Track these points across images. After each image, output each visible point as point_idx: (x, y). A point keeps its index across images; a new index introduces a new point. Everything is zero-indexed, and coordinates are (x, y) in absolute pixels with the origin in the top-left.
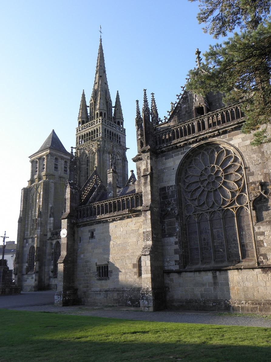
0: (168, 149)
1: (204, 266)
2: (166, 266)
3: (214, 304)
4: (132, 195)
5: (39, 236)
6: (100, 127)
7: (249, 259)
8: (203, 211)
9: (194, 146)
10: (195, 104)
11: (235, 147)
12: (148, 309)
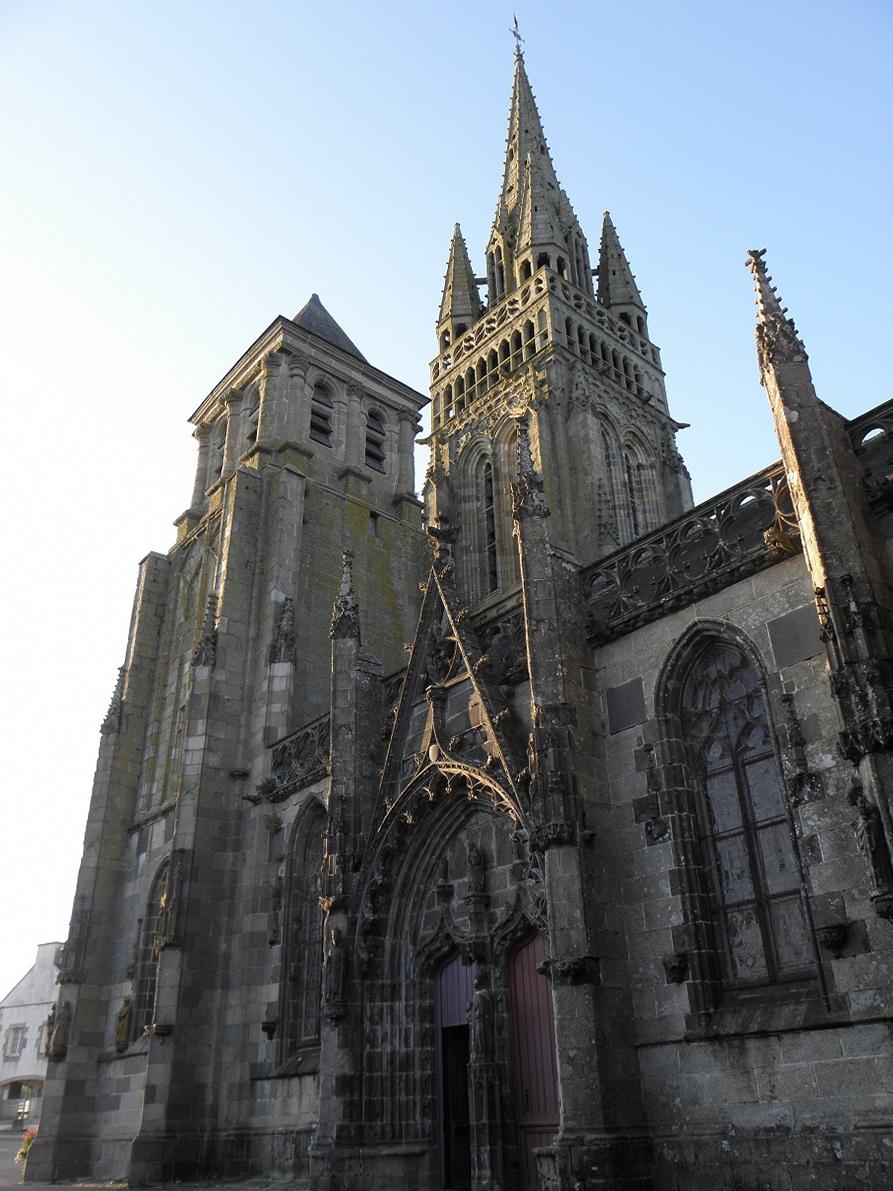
5: (196, 779)
6: (541, 310)
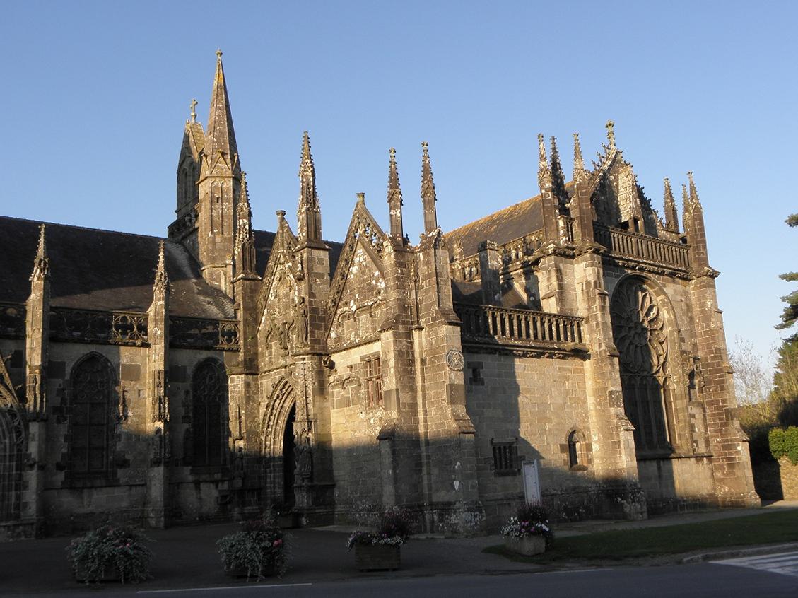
12: (641, 516)
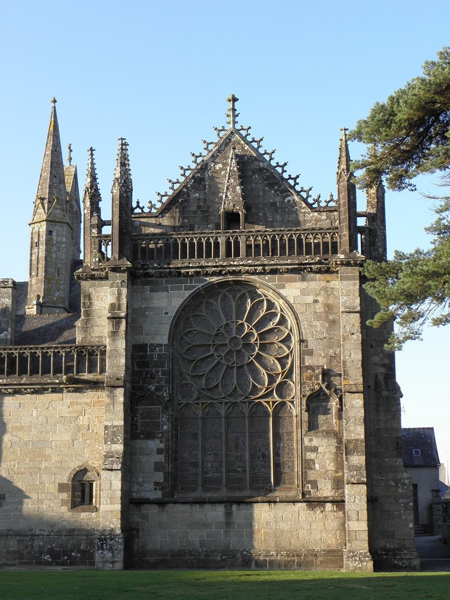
0: (161, 273)
1: (209, 495)
2: (135, 492)
3: (224, 557)
4: (71, 347)
7: (285, 488)
8: (216, 399)
9: (214, 280)
10: (225, 203)
11: (287, 302)
12: (111, 566)
